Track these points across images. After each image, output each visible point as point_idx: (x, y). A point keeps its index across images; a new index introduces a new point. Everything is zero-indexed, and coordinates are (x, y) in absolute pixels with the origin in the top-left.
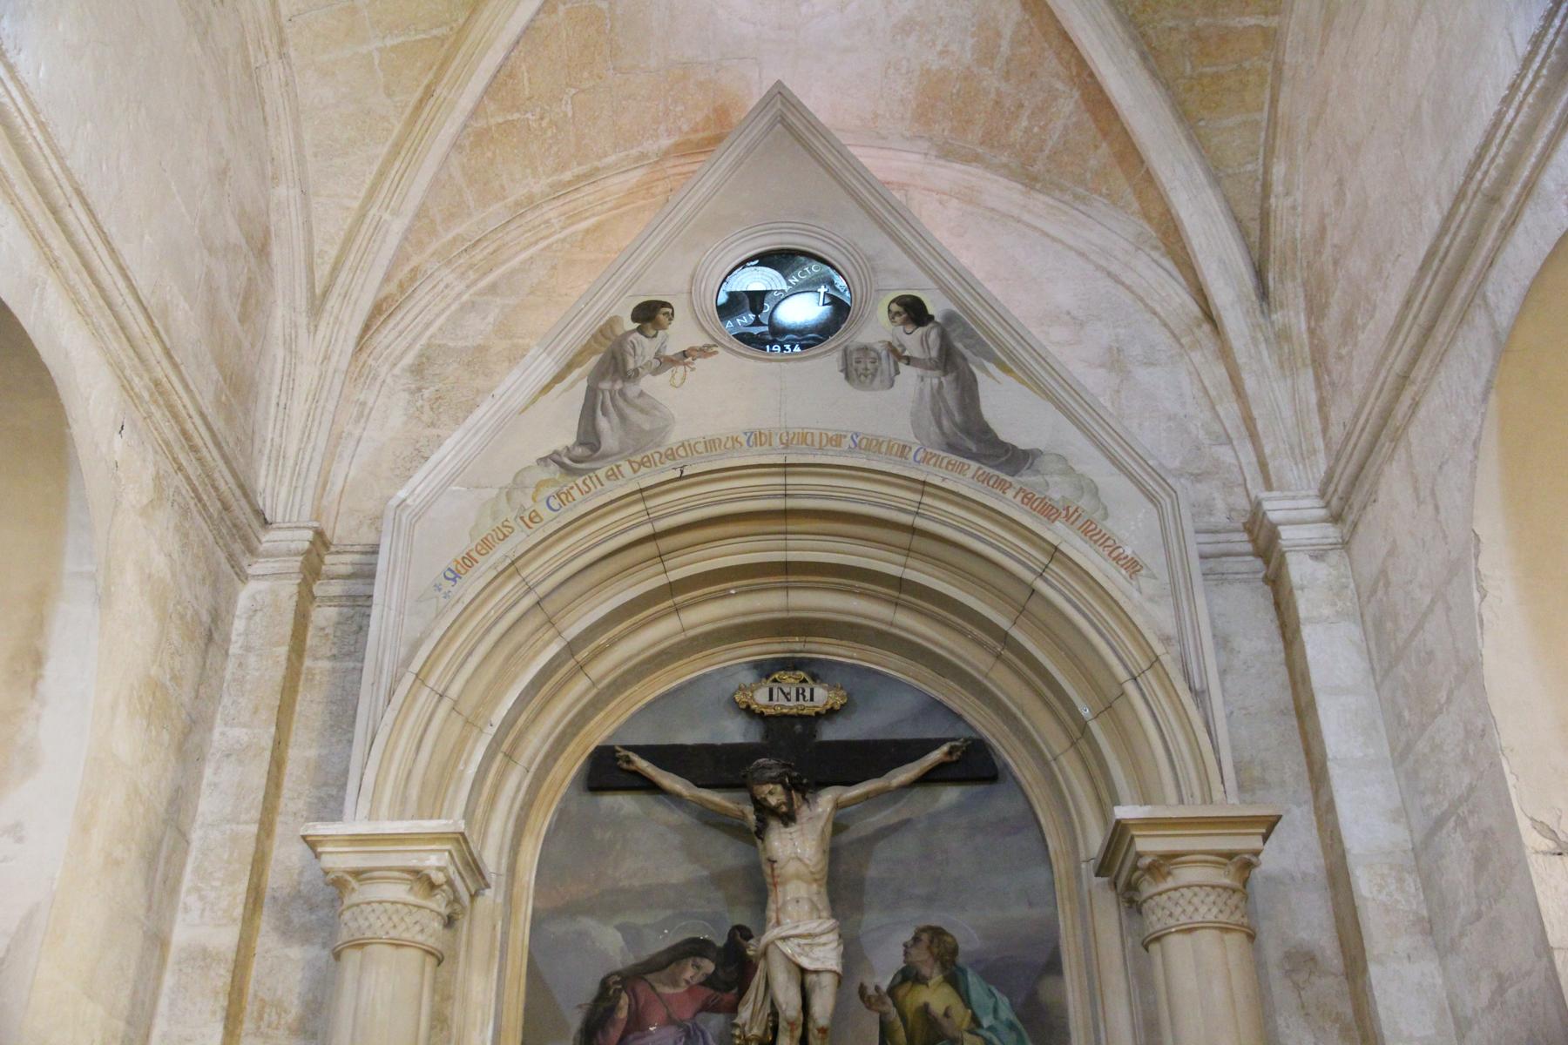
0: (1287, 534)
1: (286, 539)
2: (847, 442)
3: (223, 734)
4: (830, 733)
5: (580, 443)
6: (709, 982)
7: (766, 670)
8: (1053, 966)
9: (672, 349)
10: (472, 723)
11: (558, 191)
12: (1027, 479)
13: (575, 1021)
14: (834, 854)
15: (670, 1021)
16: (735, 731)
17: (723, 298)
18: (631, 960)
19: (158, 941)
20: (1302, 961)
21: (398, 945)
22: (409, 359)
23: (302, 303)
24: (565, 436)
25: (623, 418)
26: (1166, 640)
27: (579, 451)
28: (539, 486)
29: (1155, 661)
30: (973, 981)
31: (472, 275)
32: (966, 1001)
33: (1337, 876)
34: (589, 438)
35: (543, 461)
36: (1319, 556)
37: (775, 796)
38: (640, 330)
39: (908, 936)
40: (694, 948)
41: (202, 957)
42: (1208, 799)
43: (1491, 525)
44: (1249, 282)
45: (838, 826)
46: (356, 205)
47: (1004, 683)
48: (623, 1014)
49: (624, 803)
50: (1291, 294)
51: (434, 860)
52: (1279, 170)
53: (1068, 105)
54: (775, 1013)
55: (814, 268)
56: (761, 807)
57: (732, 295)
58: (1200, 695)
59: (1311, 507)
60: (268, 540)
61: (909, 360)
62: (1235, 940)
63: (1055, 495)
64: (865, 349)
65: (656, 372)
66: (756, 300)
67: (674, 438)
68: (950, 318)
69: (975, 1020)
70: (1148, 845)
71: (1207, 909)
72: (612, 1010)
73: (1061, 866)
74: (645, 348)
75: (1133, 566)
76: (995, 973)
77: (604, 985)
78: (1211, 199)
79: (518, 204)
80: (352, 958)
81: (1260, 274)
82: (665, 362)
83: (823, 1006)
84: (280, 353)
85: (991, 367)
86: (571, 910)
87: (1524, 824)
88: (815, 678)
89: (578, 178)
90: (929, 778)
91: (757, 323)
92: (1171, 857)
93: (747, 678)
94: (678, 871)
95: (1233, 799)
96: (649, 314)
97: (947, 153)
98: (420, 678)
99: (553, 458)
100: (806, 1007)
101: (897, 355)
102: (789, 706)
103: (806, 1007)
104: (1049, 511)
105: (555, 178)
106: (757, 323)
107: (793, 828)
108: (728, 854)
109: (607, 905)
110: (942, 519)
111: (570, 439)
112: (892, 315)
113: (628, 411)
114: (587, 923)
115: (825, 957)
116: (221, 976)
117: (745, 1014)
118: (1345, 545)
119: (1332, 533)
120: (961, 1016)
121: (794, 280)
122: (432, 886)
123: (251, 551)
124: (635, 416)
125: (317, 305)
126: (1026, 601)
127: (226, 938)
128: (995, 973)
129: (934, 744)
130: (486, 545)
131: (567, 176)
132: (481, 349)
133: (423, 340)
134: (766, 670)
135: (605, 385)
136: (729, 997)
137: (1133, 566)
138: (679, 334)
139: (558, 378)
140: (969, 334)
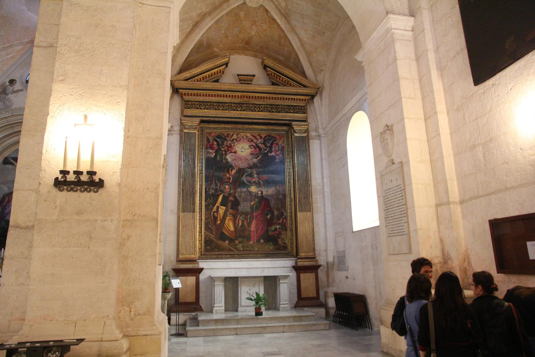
9: (15, 89)
25: (4, 102)
38: (10, 85)
48: (6, 200)
65: (12, 94)
67: (13, 107)
72: (5, 199)
74: (10, 89)
77: (4, 195)
82: (14, 92)
89: (8, 46)
96: (12, 82)
105: (3, 46)
113: (5, 101)
124: (7, 102)
131: (6, 46)
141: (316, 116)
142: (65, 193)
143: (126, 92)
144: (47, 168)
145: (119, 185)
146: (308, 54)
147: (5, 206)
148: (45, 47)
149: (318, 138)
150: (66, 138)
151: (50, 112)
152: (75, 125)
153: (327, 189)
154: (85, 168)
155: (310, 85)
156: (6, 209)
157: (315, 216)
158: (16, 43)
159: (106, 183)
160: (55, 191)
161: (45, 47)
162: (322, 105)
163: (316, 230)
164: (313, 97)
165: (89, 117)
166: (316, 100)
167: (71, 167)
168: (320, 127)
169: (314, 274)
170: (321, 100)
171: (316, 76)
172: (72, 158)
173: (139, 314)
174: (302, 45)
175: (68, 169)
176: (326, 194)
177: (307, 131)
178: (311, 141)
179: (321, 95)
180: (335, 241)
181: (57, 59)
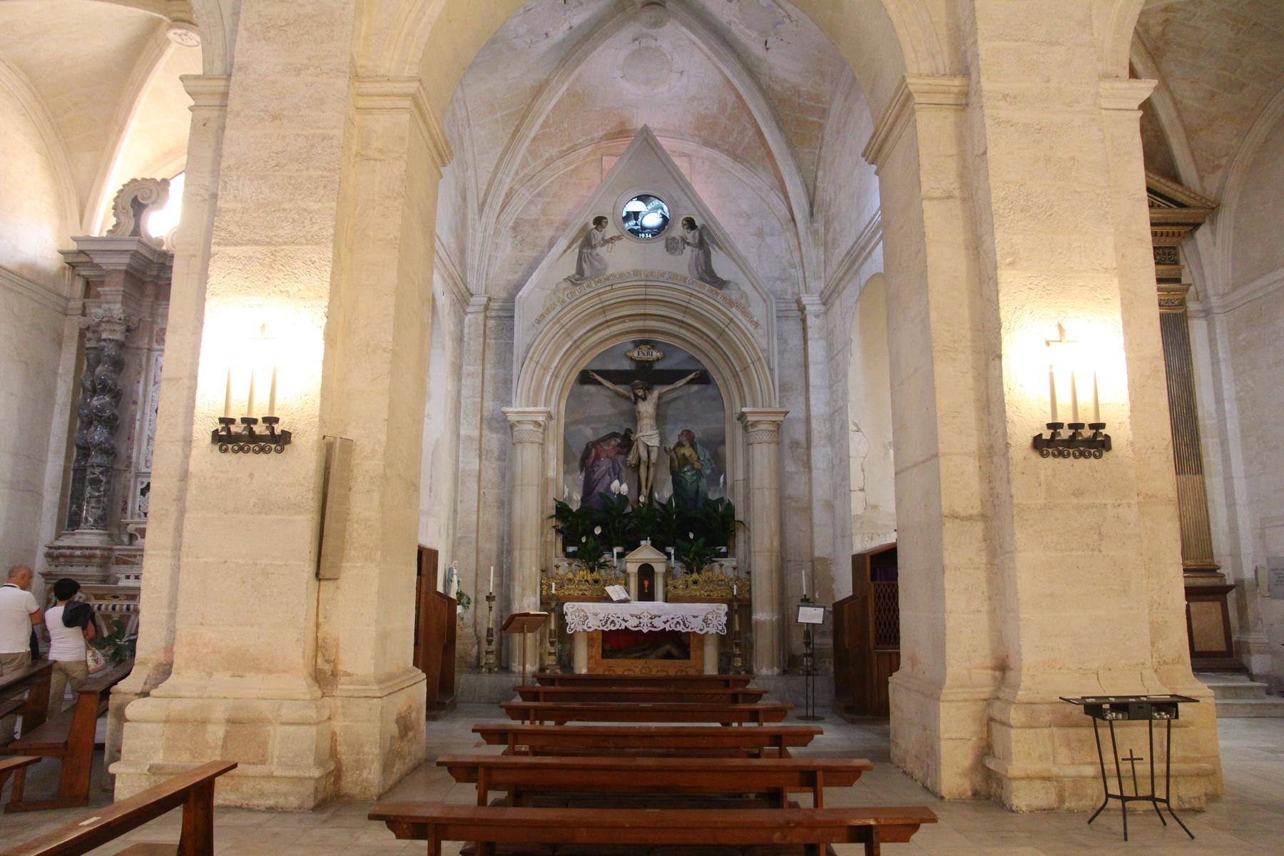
0: (808, 308)
1: (480, 300)
2: (666, 276)
3: (467, 368)
4: (657, 366)
5: (578, 273)
6: (619, 445)
7: (637, 344)
8: (723, 442)
9: (607, 237)
10: (546, 369)
11: (563, 154)
12: (725, 292)
13: (579, 456)
14: (658, 407)
15: (607, 457)
16: (626, 365)
17: (624, 214)
18: (595, 439)
19: (458, 435)
20: (795, 444)
21: (532, 443)
22: (511, 224)
23: (476, 211)
24: (572, 271)
25: (591, 264)
26: (763, 351)
27: (577, 276)
28: (565, 289)
29: (759, 359)
30: (699, 447)
31: (531, 190)
32: (696, 452)
33: (808, 420)
34: (580, 271)
35: (565, 280)
36: (817, 316)
37: (640, 393)
38: (596, 228)
39: (680, 433)
40: (614, 435)
41: (470, 439)
42: (770, 406)
43: (855, 336)
44: (807, 209)
45: (660, 398)
46: (491, 170)
47: (713, 354)
48: (593, 454)
49: (591, 388)
50: (820, 217)
51: (541, 419)
52: (820, 174)
53: (750, 132)
54: (639, 458)
55: (656, 202)
56: (636, 396)
57: (628, 213)
58: (771, 370)
59: (816, 299)
60: (473, 300)
61: (688, 244)
62: (773, 446)
63: (734, 298)
64: (674, 239)
65: (602, 246)
66: (636, 215)
67: (609, 272)
68: (703, 227)
69: (699, 458)
70: (751, 418)
71: (766, 437)
72: (590, 453)
73: (728, 412)
74: (598, 236)
75: (756, 325)
76: (706, 445)
77: (587, 446)
78: (797, 179)
79: (547, 160)
80: (519, 446)
81: (812, 205)
82: (606, 242)
83: (654, 456)
84: (471, 231)
85: (716, 247)
86: (576, 422)
87: (850, 423)
88: (653, 347)
89: (569, 148)
90: (689, 383)
91: (636, 225)
92: (758, 422)
93: (631, 346)
94: (609, 411)
95: (778, 406)
96: (599, 221)
97: (706, 143)
98: (531, 359)
99: (568, 279)
100: (649, 457)
101: (684, 241)
102: (645, 357)
103: (649, 457)
104: (731, 304)
105: (561, 149)
106: (636, 225)
107: (646, 402)
108: (625, 406)
109: (586, 421)
110: (697, 305)
111: (574, 272)
112: (683, 225)
113: (593, 261)
114: (581, 426)
115: (654, 442)
116: (476, 444)
117: (630, 457)
118: (826, 313)
119: (822, 308)
120: (694, 457)
121: (649, 207)
122: (540, 425)
123: (468, 305)
124: (596, 263)
125: (481, 211)
126: (722, 334)
127: (476, 433)
128: (706, 445)
129: (690, 372)
130: (548, 311)
131: (565, 148)
132: (536, 220)
133: (516, 216)
134: (637, 344)
135: (585, 251)
136: (625, 450)
137: (756, 325)
138: (610, 230)
139: (569, 247)
140: (709, 234)
141: (1201, 267)
142: (1050, 459)
143: (1116, 281)
144: (1015, 418)
145: (1132, 443)
146: (1190, 133)
147: (592, 466)
148: (939, 199)
149: (1202, 315)
150: (1051, 367)
151: (1003, 320)
152: (1048, 343)
153: (1233, 425)
154: (1087, 418)
155: (1193, 202)
156: (594, 473)
157: (1207, 482)
158: (581, 140)
159: (1114, 443)
160: (1034, 456)
161: (939, 199)
162: (1214, 243)
163: (1210, 511)
164: (1196, 226)
165: (1064, 327)
166: (1202, 234)
167: (1065, 417)
168: (1210, 291)
169: (1218, 604)
170: (1214, 233)
171: (1201, 179)
172: (1064, 401)
173: (1166, 663)
174: (1180, 116)
175: (1059, 420)
176: (1230, 435)
177: (1182, 303)
178: (1189, 322)
179: (1213, 223)
180: (1262, 537)
181: (996, 226)
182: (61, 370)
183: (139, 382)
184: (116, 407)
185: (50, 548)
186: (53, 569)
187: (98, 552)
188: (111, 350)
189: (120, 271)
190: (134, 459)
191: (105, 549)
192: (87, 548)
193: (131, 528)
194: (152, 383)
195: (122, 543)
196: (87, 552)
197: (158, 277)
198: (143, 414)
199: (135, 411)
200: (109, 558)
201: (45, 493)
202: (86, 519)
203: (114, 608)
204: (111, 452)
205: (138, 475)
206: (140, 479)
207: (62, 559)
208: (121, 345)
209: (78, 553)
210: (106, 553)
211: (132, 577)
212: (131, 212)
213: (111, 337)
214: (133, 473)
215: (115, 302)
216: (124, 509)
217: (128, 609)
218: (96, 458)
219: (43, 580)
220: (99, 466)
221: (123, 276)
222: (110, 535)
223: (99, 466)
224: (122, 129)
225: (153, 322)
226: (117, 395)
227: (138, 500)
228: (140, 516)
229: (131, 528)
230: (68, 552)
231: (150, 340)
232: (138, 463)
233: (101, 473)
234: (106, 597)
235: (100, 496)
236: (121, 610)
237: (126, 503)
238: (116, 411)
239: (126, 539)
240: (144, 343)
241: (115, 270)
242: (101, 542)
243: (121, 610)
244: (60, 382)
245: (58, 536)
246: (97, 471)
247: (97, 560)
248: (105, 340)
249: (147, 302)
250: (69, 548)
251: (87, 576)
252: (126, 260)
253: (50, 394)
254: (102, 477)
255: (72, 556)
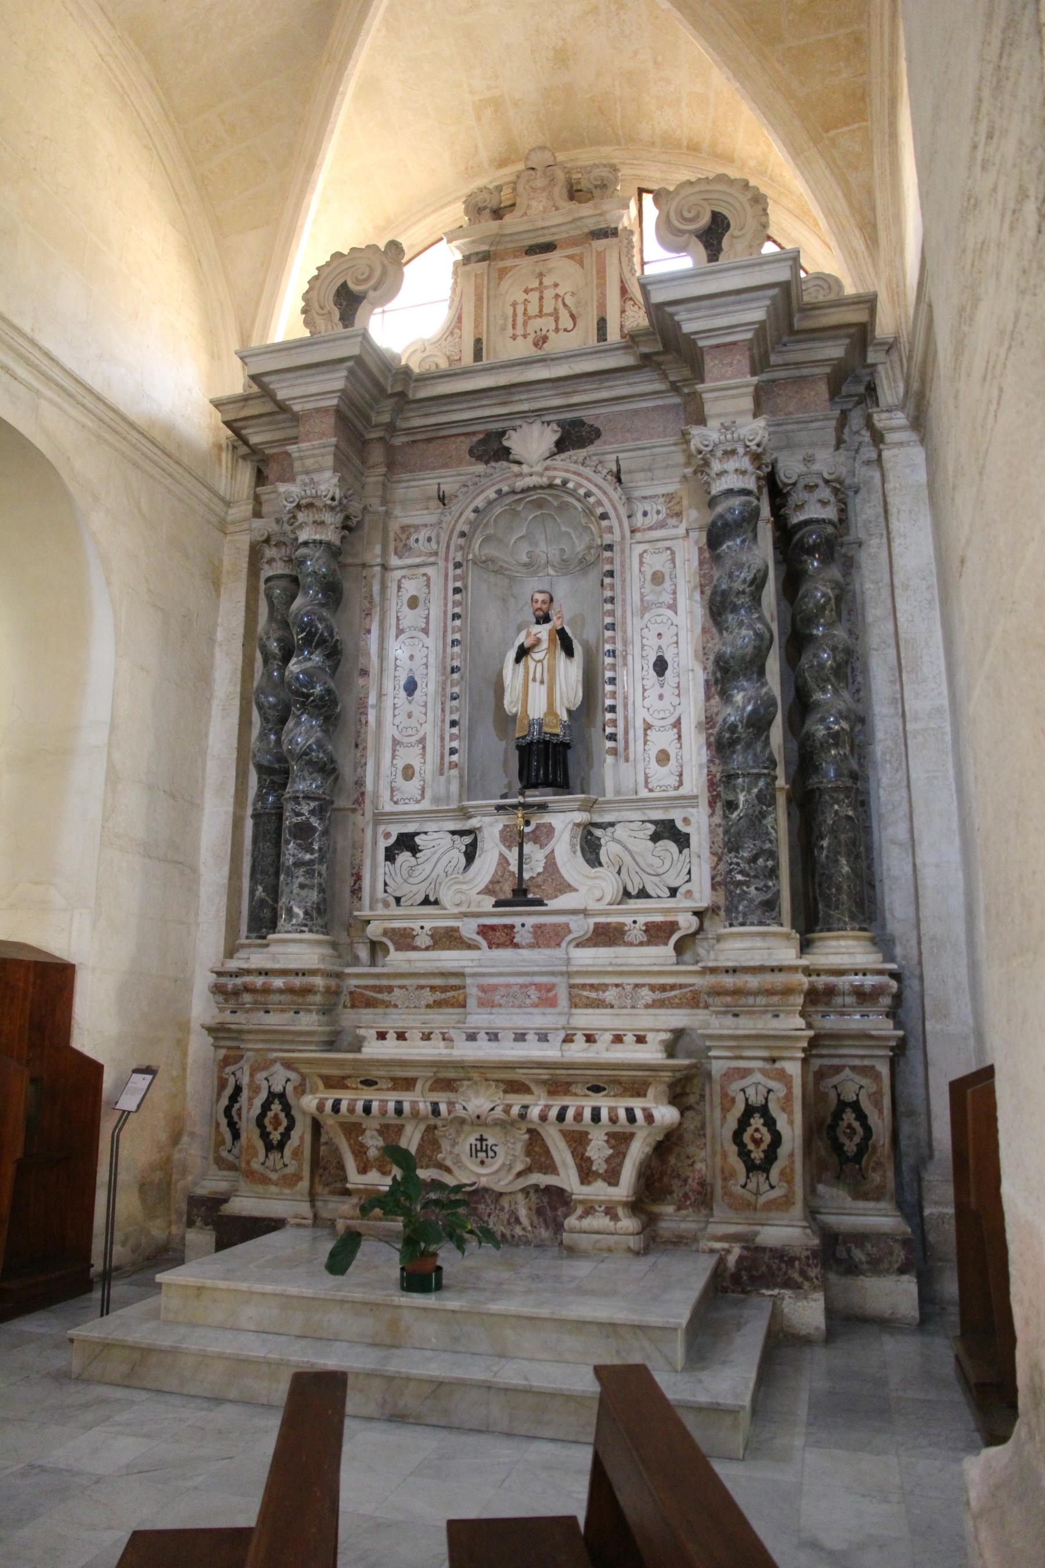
182: (220, 635)
183: (369, 631)
184: (333, 675)
185: (219, 974)
186: (227, 1017)
187: (319, 981)
188: (315, 563)
189: (325, 410)
190: (369, 786)
191: (329, 975)
192: (297, 973)
193: (374, 930)
194: (393, 632)
195: (356, 961)
196: (297, 982)
197: (391, 428)
198: (380, 696)
199: (366, 689)
200: (337, 993)
201: (202, 869)
202: (290, 911)
203: (367, 1109)
204: (328, 769)
205: (379, 818)
206: (381, 829)
207: (247, 998)
208: (334, 552)
209: (278, 982)
210: (333, 983)
211: (391, 1035)
212: (337, 314)
213: (317, 537)
214: (369, 814)
215: (321, 470)
216: (356, 891)
217: (399, 1111)
218: (303, 784)
219: (212, 1040)
220: (307, 797)
221: (331, 420)
222: (334, 945)
223: (307, 797)
224: (311, 165)
225: (388, 514)
226: (334, 653)
227: (381, 871)
228: (386, 905)
229: (374, 930)
230: (259, 981)
231: (385, 553)
232: (376, 795)
233: (312, 812)
234: (348, 1082)
235: (311, 862)
236: (384, 1113)
237: (358, 878)
238: (332, 685)
239: (364, 953)
240: (374, 554)
241: (318, 410)
242: (323, 959)
243: (384, 1113)
244: (219, 654)
245: (230, 952)
246: (305, 808)
247: (318, 998)
248: (305, 544)
249: (374, 478)
250: (261, 972)
251: (295, 1033)
252: (336, 380)
253: (204, 677)
254: (315, 822)
255: (266, 990)
